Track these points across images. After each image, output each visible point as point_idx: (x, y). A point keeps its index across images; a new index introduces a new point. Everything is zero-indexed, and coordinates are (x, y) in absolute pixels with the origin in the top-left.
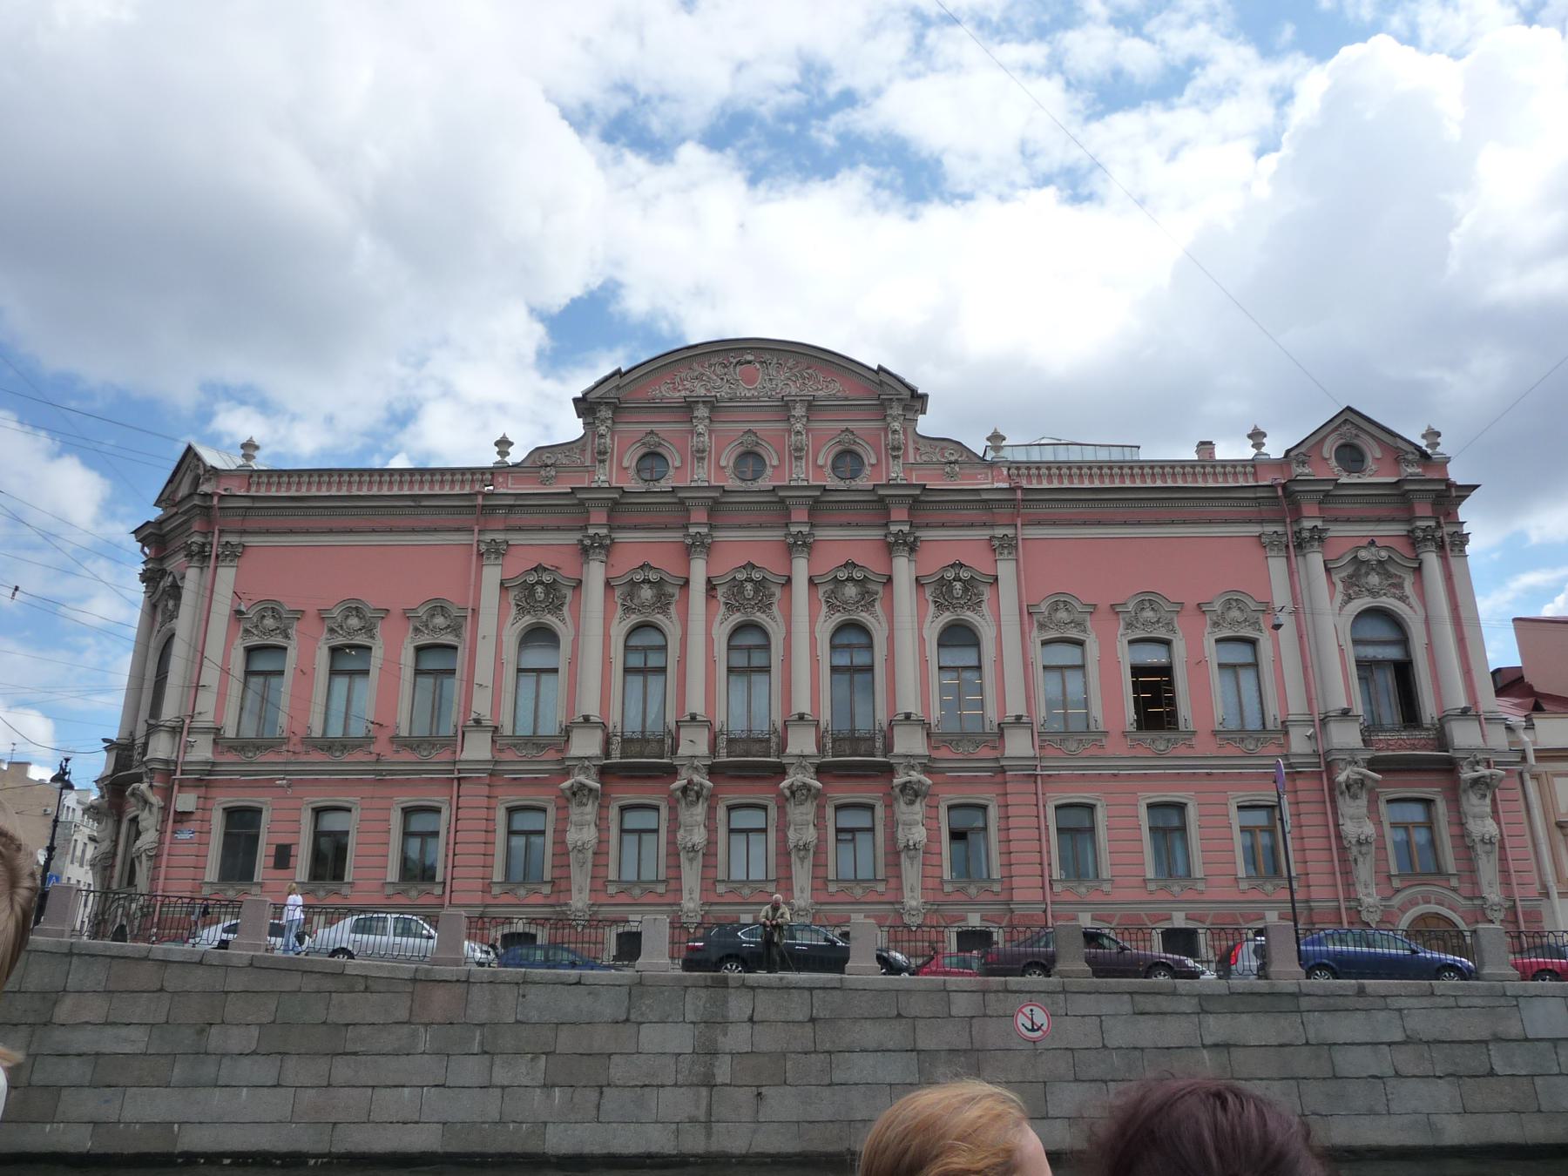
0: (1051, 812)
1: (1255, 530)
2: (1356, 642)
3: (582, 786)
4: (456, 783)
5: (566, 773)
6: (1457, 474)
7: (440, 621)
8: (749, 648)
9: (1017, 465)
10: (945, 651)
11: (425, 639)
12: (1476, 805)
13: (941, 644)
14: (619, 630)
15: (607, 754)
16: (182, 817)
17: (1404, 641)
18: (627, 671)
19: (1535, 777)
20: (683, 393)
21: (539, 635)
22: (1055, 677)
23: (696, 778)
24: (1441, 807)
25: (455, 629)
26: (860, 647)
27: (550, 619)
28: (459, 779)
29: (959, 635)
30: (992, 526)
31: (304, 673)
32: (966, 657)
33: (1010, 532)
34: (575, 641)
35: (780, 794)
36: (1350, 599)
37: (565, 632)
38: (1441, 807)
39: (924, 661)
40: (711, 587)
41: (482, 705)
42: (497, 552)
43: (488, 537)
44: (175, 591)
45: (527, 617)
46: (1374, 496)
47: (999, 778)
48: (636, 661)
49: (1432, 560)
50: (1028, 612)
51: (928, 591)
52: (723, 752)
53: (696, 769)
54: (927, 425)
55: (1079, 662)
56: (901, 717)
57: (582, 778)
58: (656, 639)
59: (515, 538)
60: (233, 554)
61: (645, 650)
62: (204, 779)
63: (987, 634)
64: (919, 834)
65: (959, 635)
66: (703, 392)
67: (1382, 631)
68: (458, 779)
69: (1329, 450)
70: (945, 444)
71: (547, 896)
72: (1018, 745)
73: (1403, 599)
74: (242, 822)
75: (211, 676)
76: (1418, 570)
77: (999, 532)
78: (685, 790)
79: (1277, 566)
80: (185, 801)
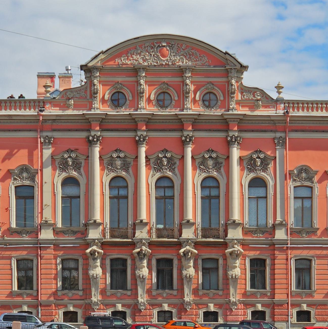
0: (293, 262)
3: (95, 251)
4: (39, 248)
5: (88, 245)
7: (25, 175)
8: (165, 187)
9: (289, 102)
10: (253, 190)
11: (19, 183)
15: (104, 236)
20: (132, 61)
21: (69, 182)
22: (300, 201)
23: (144, 248)
25: (32, 179)
26: (214, 187)
28: (40, 247)
30: (275, 131)
32: (260, 192)
33: (283, 135)
35: (179, 254)
37: (82, 181)
39: (242, 195)
41: (47, 214)
42: (49, 142)
45: (64, 173)
47: (272, 248)
51: (245, 163)
52: (154, 236)
53: (144, 244)
54: (249, 79)
55: (310, 196)
56: (232, 221)
57: (95, 248)
58: (122, 184)
59: (57, 135)
61: (119, 188)
63: (271, 183)
64: (237, 272)
65: (257, 183)
66: (141, 61)
68: (39, 246)
70: (256, 90)
71: (81, 296)
72: (280, 235)
77: (278, 135)
78: (139, 253)
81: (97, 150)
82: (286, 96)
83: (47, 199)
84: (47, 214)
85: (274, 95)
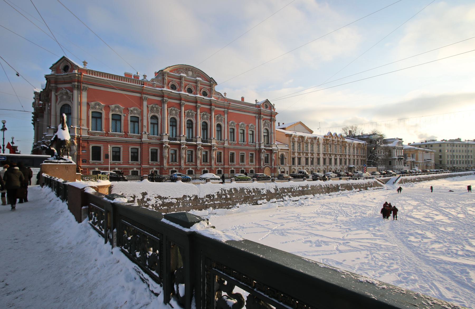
1: (254, 115)
12: (274, 155)
14: (169, 119)
16: (83, 147)
27: (156, 114)
29: (219, 126)
31: (107, 119)
43: (144, 96)
60: (86, 89)
62: (87, 141)
75: (84, 116)
79: (257, 120)
80: (85, 144)
83: (145, 123)
84: (145, 129)
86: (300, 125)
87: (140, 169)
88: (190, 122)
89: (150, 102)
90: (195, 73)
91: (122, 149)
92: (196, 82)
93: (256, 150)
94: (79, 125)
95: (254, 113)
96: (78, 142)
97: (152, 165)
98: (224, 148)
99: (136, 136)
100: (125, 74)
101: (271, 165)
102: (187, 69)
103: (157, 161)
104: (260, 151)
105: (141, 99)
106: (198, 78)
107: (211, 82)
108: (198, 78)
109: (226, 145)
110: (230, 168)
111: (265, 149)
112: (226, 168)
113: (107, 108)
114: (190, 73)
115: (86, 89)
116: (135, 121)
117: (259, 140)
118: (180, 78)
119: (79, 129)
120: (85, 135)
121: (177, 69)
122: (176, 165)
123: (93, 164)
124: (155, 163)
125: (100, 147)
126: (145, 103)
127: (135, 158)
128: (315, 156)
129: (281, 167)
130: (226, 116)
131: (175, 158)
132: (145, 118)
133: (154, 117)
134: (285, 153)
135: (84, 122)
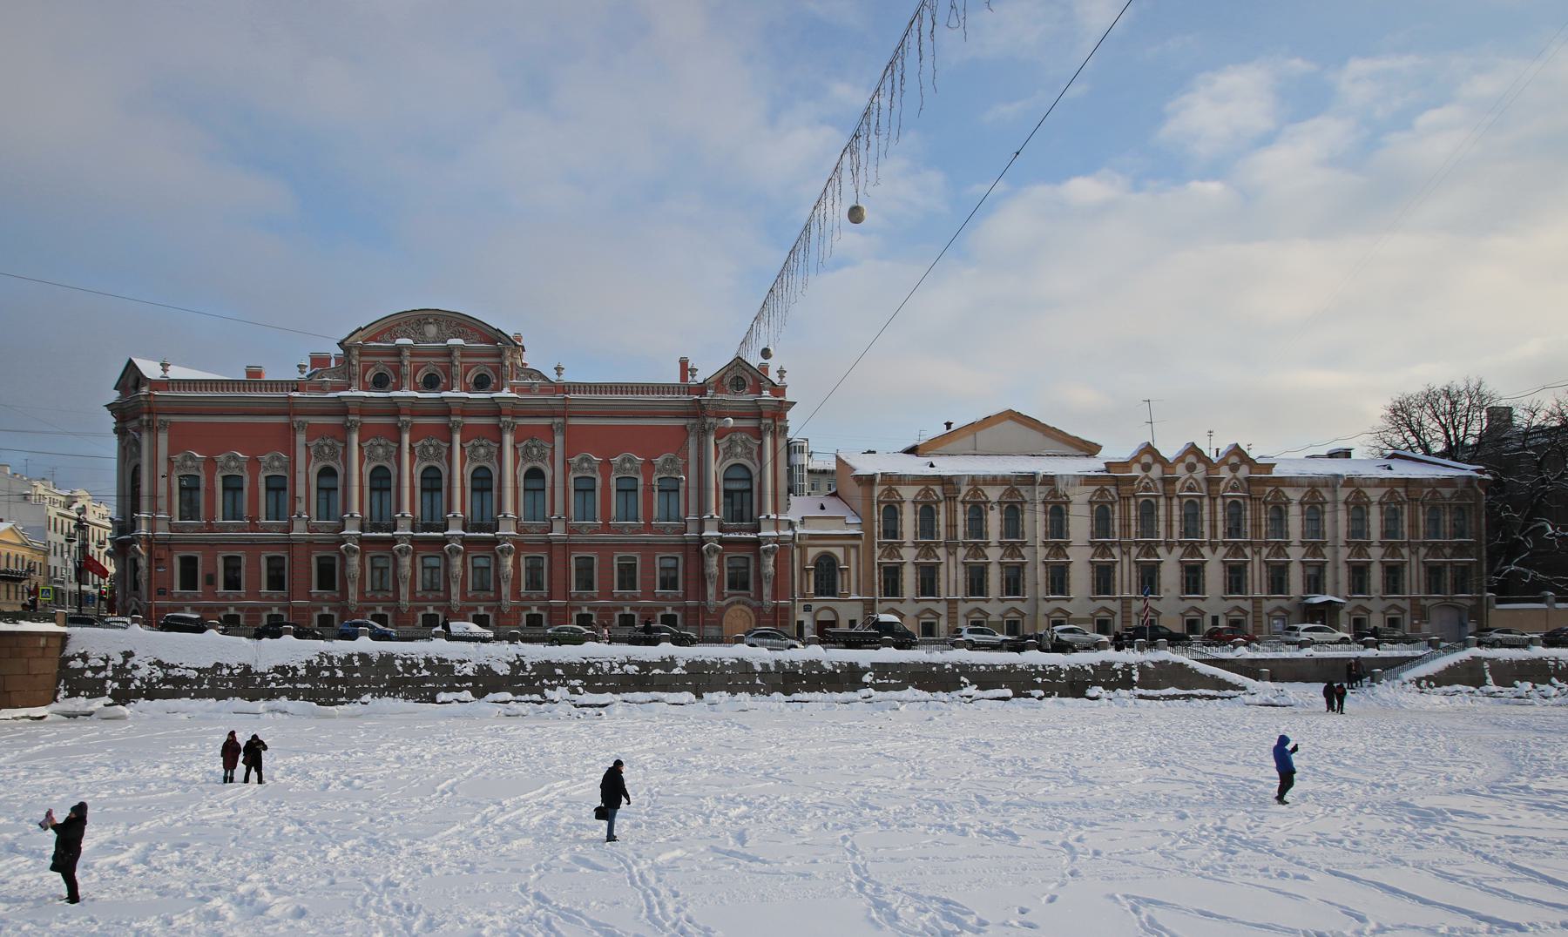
2: (725, 479)
6: (789, 398)
13: (526, 477)
16: (159, 560)
17: (750, 479)
18: (372, 489)
19: (799, 546)
24: (752, 562)
29: (535, 474)
31: (211, 491)
32: (535, 484)
33: (561, 420)
34: (345, 475)
36: (724, 459)
37: (340, 471)
38: (752, 562)
40: (412, 448)
43: (298, 418)
44: (138, 444)
46: (746, 402)
48: (377, 484)
49: (768, 440)
50: (567, 466)
62: (168, 544)
63: (548, 473)
65: (535, 474)
67: (740, 474)
69: (727, 380)
73: (752, 459)
74: (189, 565)
76: (761, 447)
77: (557, 420)
80: (163, 554)
81: (355, 438)
82: (567, 378)
84: (300, 507)
85: (553, 377)
86: (1009, 424)
87: (286, 609)
88: (431, 474)
89: (313, 432)
90: (448, 327)
91: (244, 560)
92: (449, 352)
93: (684, 545)
94: (154, 509)
95: (677, 416)
96: (150, 551)
97: (319, 598)
98: (549, 542)
99: (278, 525)
100: (249, 374)
101: (760, 596)
102: (417, 320)
103: (333, 588)
104: (695, 550)
105: (290, 430)
106: (451, 342)
107: (500, 345)
108: (451, 342)
109: (558, 532)
110: (573, 609)
111: (721, 541)
112: (559, 608)
113: (211, 463)
114: (431, 330)
115: (164, 425)
116: (277, 486)
117: (702, 508)
118: (398, 351)
119: (152, 521)
120: (162, 532)
121: (390, 329)
122: (387, 600)
123: (225, 598)
124: (326, 594)
125: (195, 559)
126: (301, 438)
127: (276, 582)
128: (1036, 557)
129: (815, 606)
130: (559, 439)
131: (386, 577)
132: (301, 479)
133: (328, 472)
134: (839, 553)
135: (162, 503)
